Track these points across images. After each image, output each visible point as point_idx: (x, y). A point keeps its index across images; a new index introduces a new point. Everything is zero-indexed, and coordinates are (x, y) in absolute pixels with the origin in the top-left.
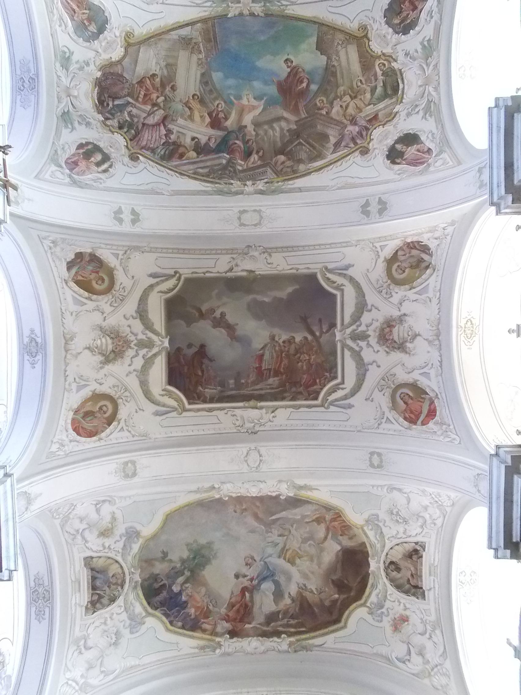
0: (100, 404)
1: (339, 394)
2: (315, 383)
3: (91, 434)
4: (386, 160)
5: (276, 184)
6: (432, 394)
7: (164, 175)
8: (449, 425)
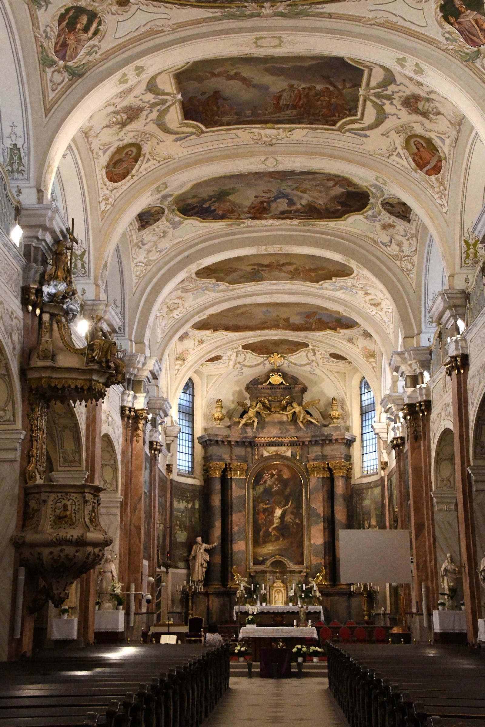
0: (125, 152)
1: (357, 126)
2: (334, 115)
3: (124, 176)
4: (438, 10)
5: (301, 7)
6: (442, 154)
7: (163, 10)
8: (446, 190)
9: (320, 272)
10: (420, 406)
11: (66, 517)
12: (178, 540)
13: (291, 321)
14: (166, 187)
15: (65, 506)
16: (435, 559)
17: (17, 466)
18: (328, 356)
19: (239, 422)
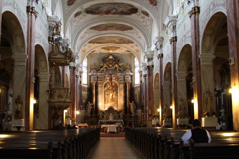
3: (72, 4)
9: (124, 28)
10: (151, 66)
11: (61, 96)
12: (83, 102)
13: (116, 41)
14: (83, 7)
15: (60, 93)
16: (153, 107)
17: (48, 83)
18: (126, 51)
19: (100, 70)
